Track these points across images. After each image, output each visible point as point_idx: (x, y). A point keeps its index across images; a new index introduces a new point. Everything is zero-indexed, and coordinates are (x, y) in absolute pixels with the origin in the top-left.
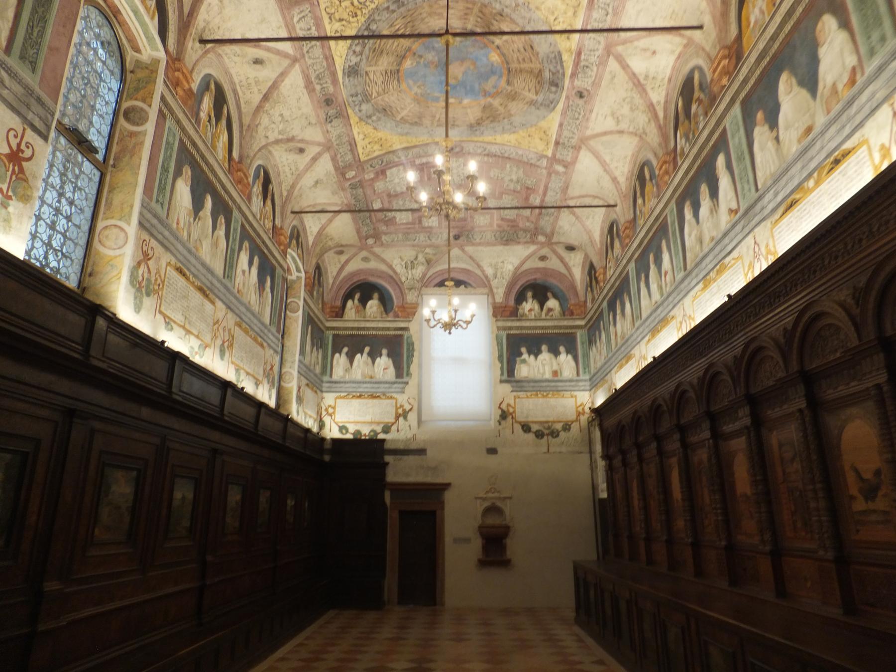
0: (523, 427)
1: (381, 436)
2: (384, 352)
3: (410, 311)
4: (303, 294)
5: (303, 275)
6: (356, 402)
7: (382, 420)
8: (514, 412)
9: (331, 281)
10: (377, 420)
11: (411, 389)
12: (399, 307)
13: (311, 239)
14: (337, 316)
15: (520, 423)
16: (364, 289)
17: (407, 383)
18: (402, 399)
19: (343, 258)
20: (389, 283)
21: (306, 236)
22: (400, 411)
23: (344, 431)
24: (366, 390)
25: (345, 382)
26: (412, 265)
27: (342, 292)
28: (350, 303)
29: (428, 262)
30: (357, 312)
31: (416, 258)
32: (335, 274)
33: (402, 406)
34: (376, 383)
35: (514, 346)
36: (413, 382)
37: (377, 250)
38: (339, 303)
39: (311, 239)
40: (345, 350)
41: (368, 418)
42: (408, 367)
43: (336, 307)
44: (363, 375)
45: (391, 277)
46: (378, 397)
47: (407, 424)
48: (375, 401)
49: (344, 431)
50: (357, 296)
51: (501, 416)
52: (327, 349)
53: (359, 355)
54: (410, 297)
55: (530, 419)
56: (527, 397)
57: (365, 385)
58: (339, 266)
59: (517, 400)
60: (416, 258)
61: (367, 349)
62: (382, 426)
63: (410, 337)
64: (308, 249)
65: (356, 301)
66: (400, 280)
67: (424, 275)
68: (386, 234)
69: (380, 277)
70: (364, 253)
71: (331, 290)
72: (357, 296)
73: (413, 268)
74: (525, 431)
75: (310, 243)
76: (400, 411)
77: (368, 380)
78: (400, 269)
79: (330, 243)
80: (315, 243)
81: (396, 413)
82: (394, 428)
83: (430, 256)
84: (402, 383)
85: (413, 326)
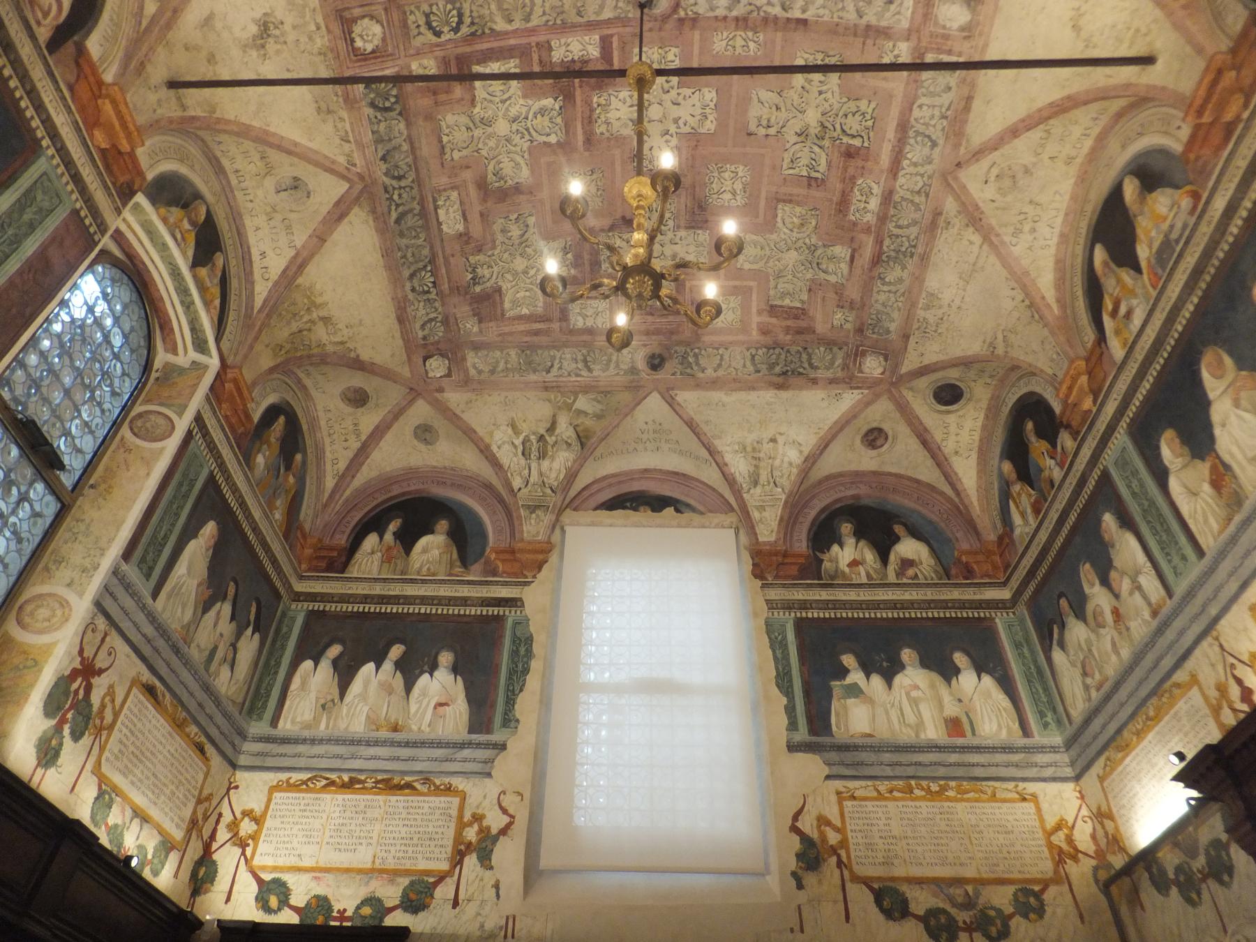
0: (879, 896)
1: (396, 919)
2: (446, 658)
3: (532, 560)
4: (197, 401)
5: (214, 362)
6: (333, 802)
7: (408, 865)
8: (844, 843)
9: (330, 483)
10: (391, 864)
11: (512, 767)
12: (499, 552)
13: (261, 290)
14: (328, 570)
15: (866, 882)
16: (412, 512)
17: (503, 747)
18: (481, 795)
19: (368, 420)
20: (482, 500)
21: (250, 282)
22: (471, 834)
23: (273, 902)
24: (372, 765)
25: (313, 741)
26: (538, 447)
27: (357, 516)
28: (371, 540)
29: (583, 439)
30: (388, 559)
31: (552, 429)
32: (342, 465)
33: (477, 818)
34: (407, 744)
35: (817, 655)
36: (520, 743)
37: (454, 398)
38: (342, 540)
39: (261, 290)
40: (335, 650)
41: (363, 857)
42: (510, 702)
43: (332, 549)
44: (372, 722)
45: (489, 487)
46: (409, 786)
47: (489, 877)
48: (397, 801)
49: (273, 902)
50: (393, 527)
51: (799, 856)
52: (283, 647)
53: (370, 666)
54: (533, 528)
55: (899, 871)
56: (880, 797)
57: (372, 751)
58: (355, 445)
59: (848, 804)
60: (552, 429)
61: (396, 651)
62: (405, 881)
63: (523, 623)
64: (248, 316)
65: (389, 537)
66: (508, 485)
67: (571, 476)
68: (476, 347)
69: (460, 487)
70: (421, 411)
71: (325, 506)
72: (393, 527)
73: (542, 455)
74: (888, 914)
75: (258, 302)
76: (471, 834)
77: (384, 734)
78: (506, 456)
79: (321, 333)
80: (274, 306)
81: (458, 838)
82: (444, 892)
83: (588, 422)
84: (487, 745)
85: (534, 597)
